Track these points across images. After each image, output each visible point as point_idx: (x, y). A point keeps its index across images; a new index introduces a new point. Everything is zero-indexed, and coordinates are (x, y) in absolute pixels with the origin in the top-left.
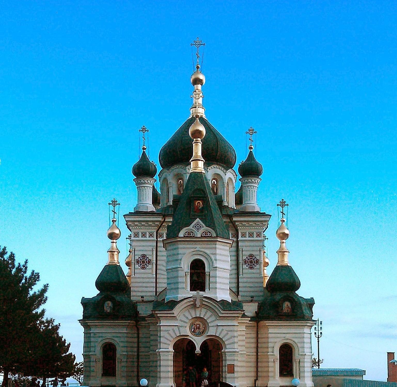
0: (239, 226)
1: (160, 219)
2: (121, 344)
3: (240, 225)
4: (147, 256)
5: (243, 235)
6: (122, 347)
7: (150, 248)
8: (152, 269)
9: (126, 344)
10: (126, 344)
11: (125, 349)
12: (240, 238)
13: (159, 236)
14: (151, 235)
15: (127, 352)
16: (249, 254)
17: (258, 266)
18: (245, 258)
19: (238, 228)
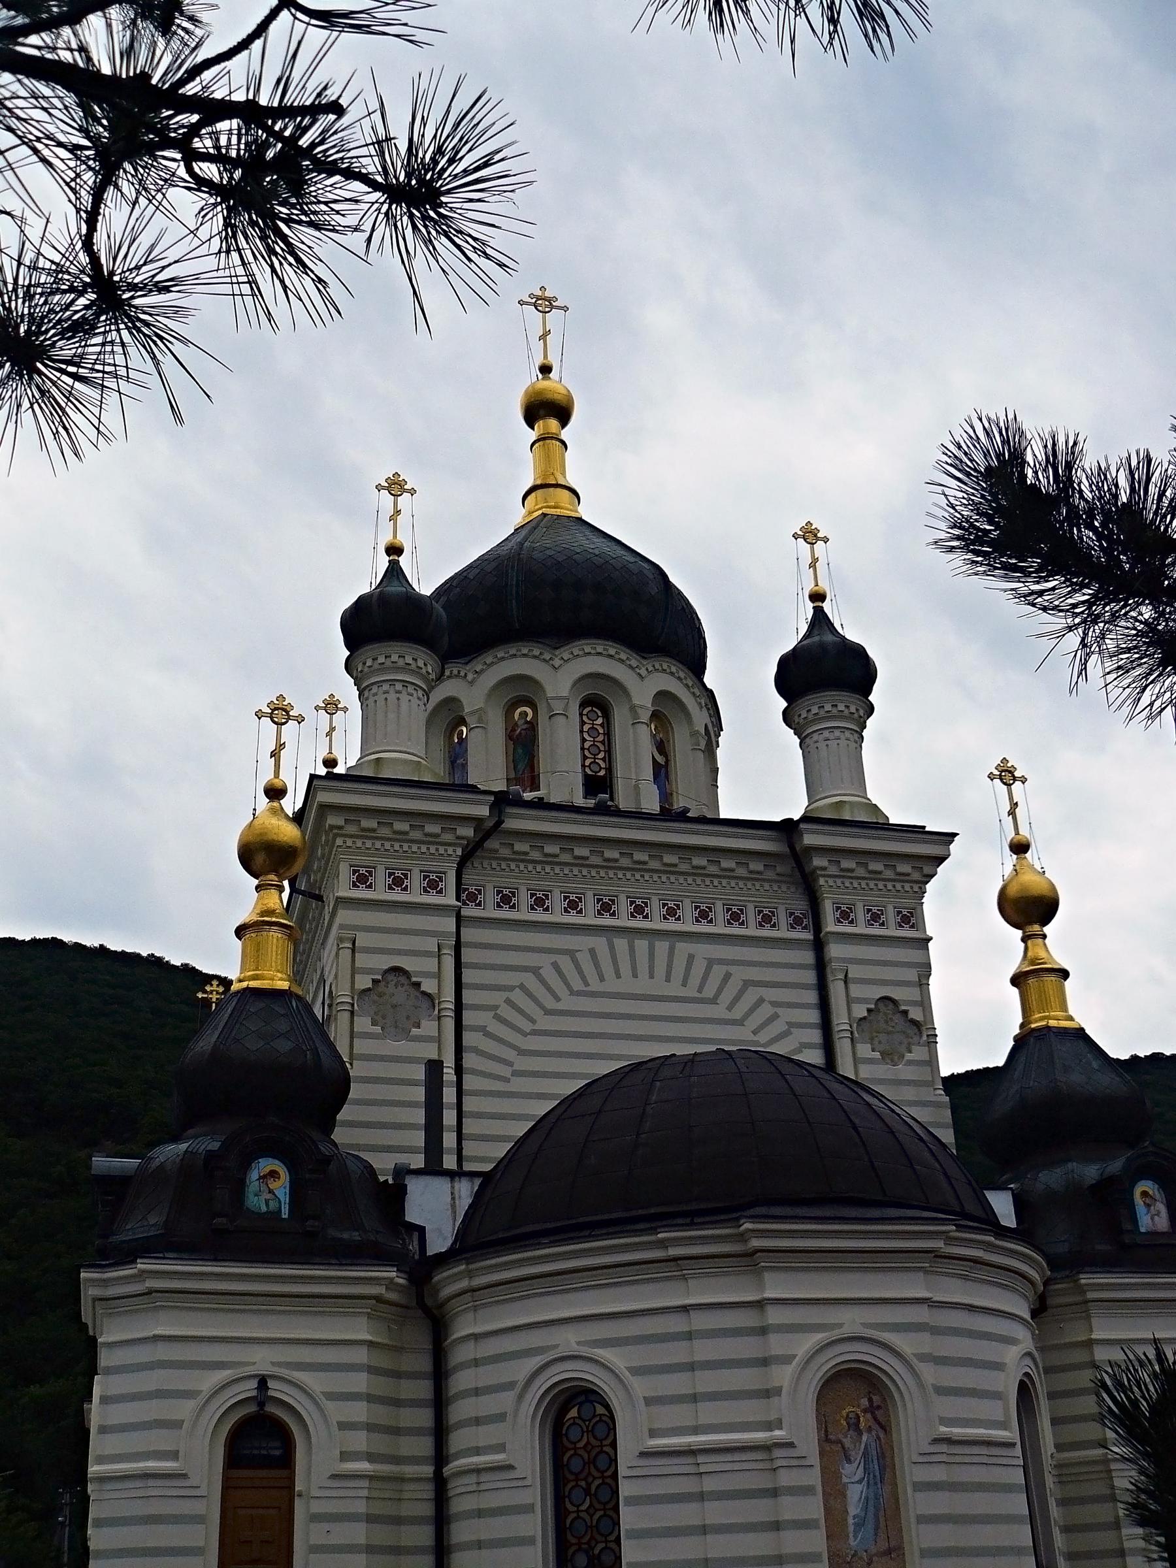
0: (824, 876)
1: (484, 811)
2: (338, 1411)
3: (833, 870)
4: (414, 979)
5: (845, 916)
6: (343, 1426)
7: (431, 944)
8: (439, 1040)
9: (359, 1412)
10: (359, 1412)
11: (359, 1441)
12: (830, 925)
13: (464, 896)
14: (433, 885)
15: (371, 1457)
16: (878, 997)
17: (918, 1053)
18: (860, 1011)
19: (822, 881)
